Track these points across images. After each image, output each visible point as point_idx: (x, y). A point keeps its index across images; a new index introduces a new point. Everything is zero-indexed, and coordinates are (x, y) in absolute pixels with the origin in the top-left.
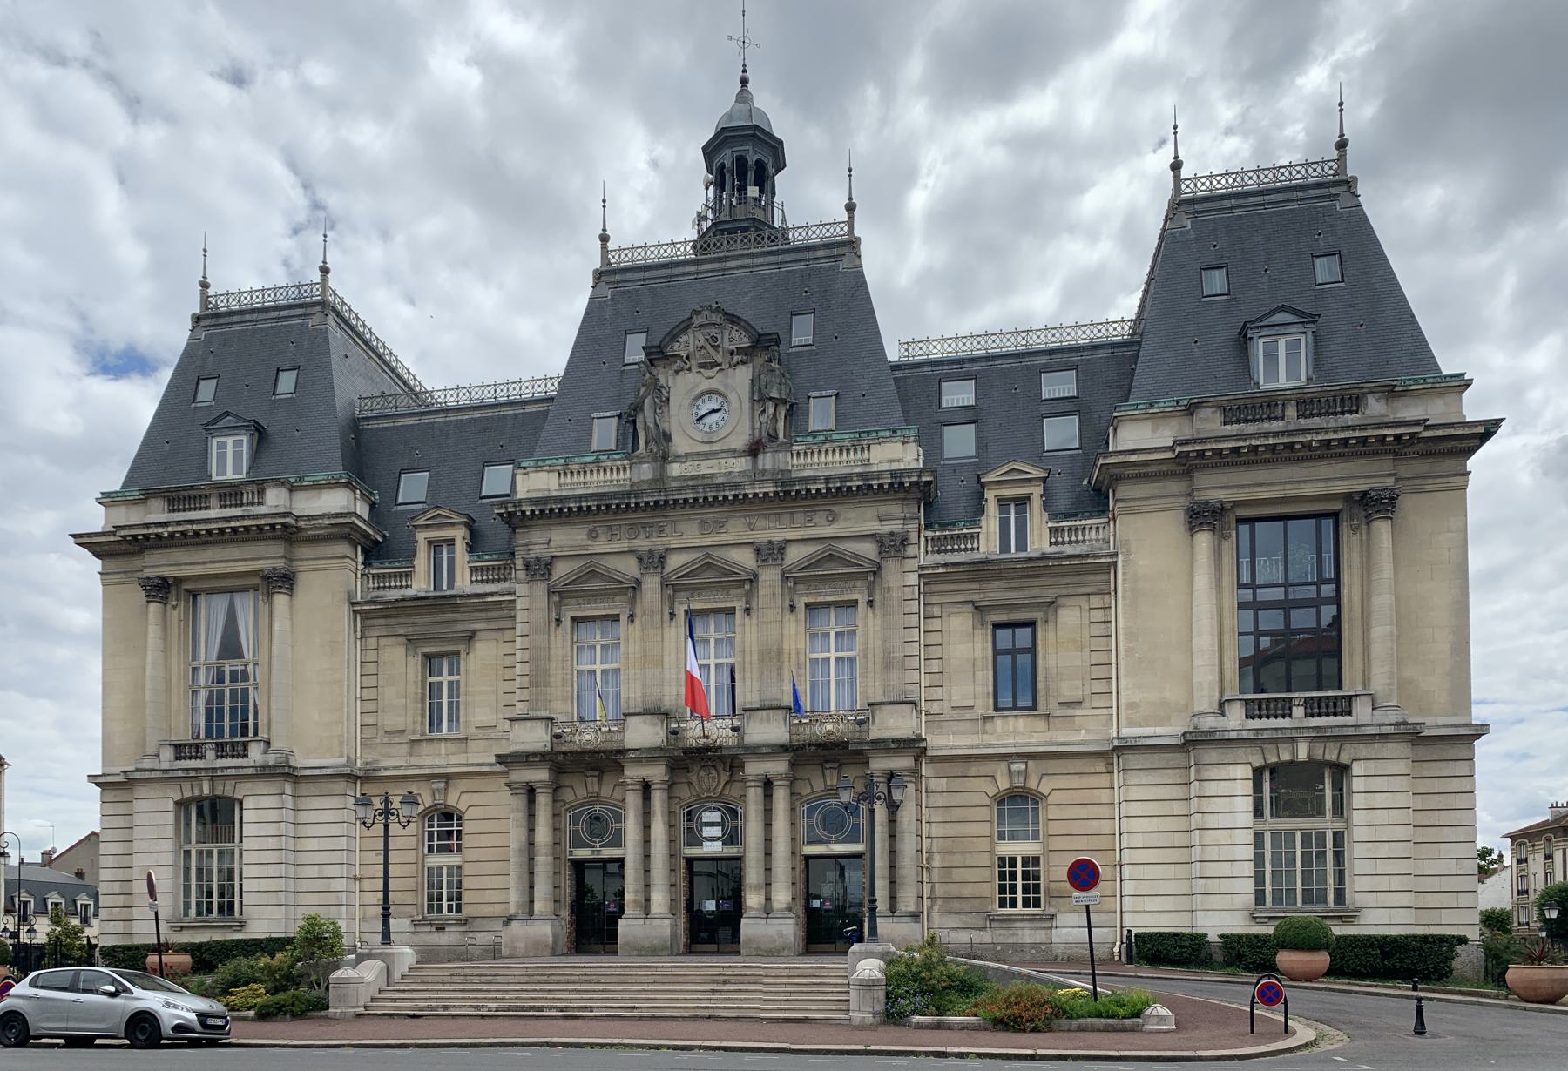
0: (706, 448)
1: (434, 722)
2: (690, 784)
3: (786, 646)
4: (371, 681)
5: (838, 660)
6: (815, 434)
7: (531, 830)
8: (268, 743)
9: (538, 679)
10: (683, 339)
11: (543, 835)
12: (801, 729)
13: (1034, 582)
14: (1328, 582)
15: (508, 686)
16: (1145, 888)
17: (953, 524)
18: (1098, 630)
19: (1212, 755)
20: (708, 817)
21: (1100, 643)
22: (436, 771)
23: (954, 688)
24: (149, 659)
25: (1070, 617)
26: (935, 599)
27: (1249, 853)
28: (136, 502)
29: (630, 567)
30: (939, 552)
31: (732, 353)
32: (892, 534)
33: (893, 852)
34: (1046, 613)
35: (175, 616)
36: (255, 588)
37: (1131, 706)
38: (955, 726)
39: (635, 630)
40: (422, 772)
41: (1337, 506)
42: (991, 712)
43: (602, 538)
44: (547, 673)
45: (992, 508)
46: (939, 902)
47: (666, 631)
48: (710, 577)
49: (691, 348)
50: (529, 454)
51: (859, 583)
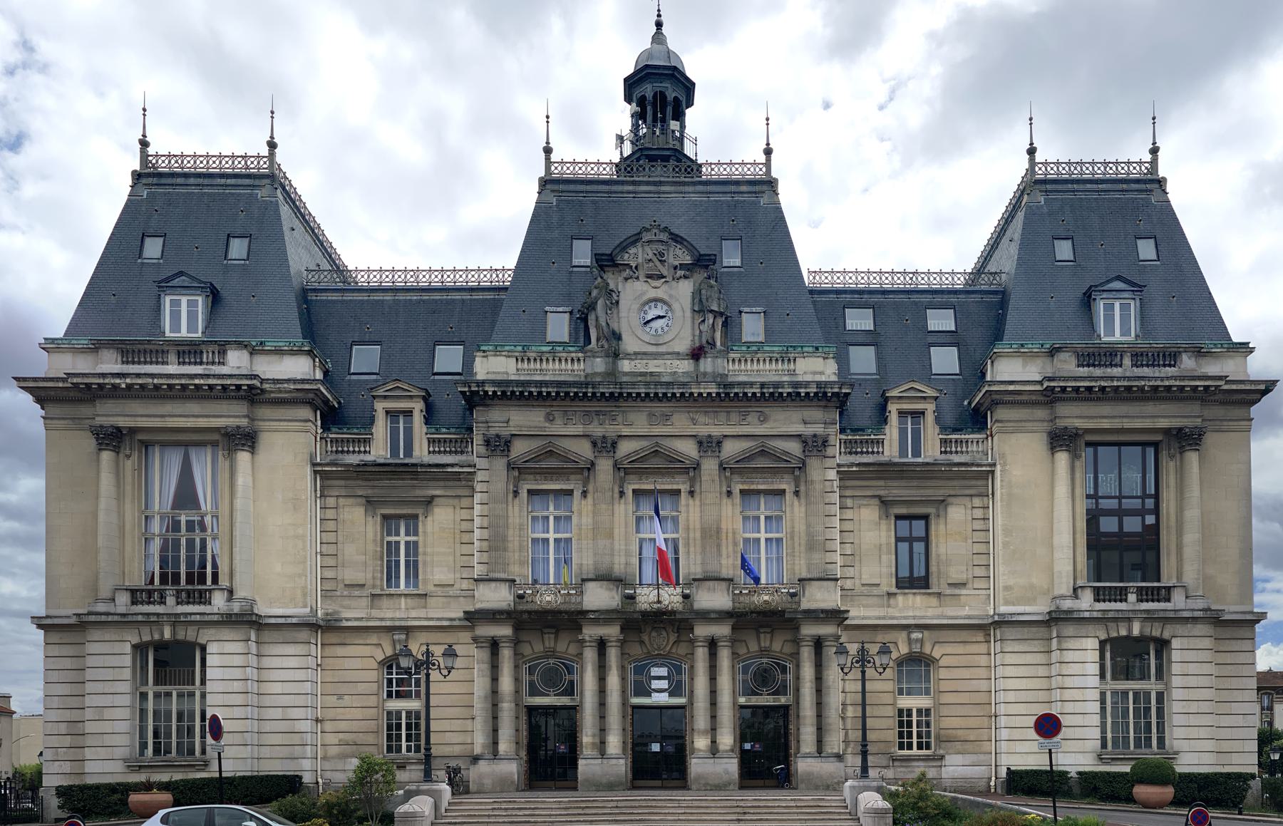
1: (392, 577)
2: (642, 642)
3: (724, 526)
4: (331, 537)
5: (767, 540)
7: (495, 679)
8: (231, 592)
10: (632, 251)
12: (742, 599)
13: (929, 483)
14: (1150, 496)
17: (863, 430)
18: (978, 525)
19: (1069, 630)
20: (655, 671)
21: (979, 536)
22: (397, 623)
23: (864, 569)
24: (103, 504)
25: (958, 514)
26: (848, 493)
27: (1096, 707)
28: (83, 351)
29: (584, 450)
30: (850, 453)
31: (675, 268)
32: (815, 436)
33: (819, 705)
34: (938, 509)
35: (129, 463)
36: (214, 444)
37: (1007, 588)
38: (865, 601)
40: (383, 624)
41: (1158, 437)
42: (894, 590)
43: (559, 421)
44: (504, 539)
45: (894, 418)
46: (852, 745)
47: (616, 506)
48: (656, 463)
49: (640, 260)
50: (487, 340)
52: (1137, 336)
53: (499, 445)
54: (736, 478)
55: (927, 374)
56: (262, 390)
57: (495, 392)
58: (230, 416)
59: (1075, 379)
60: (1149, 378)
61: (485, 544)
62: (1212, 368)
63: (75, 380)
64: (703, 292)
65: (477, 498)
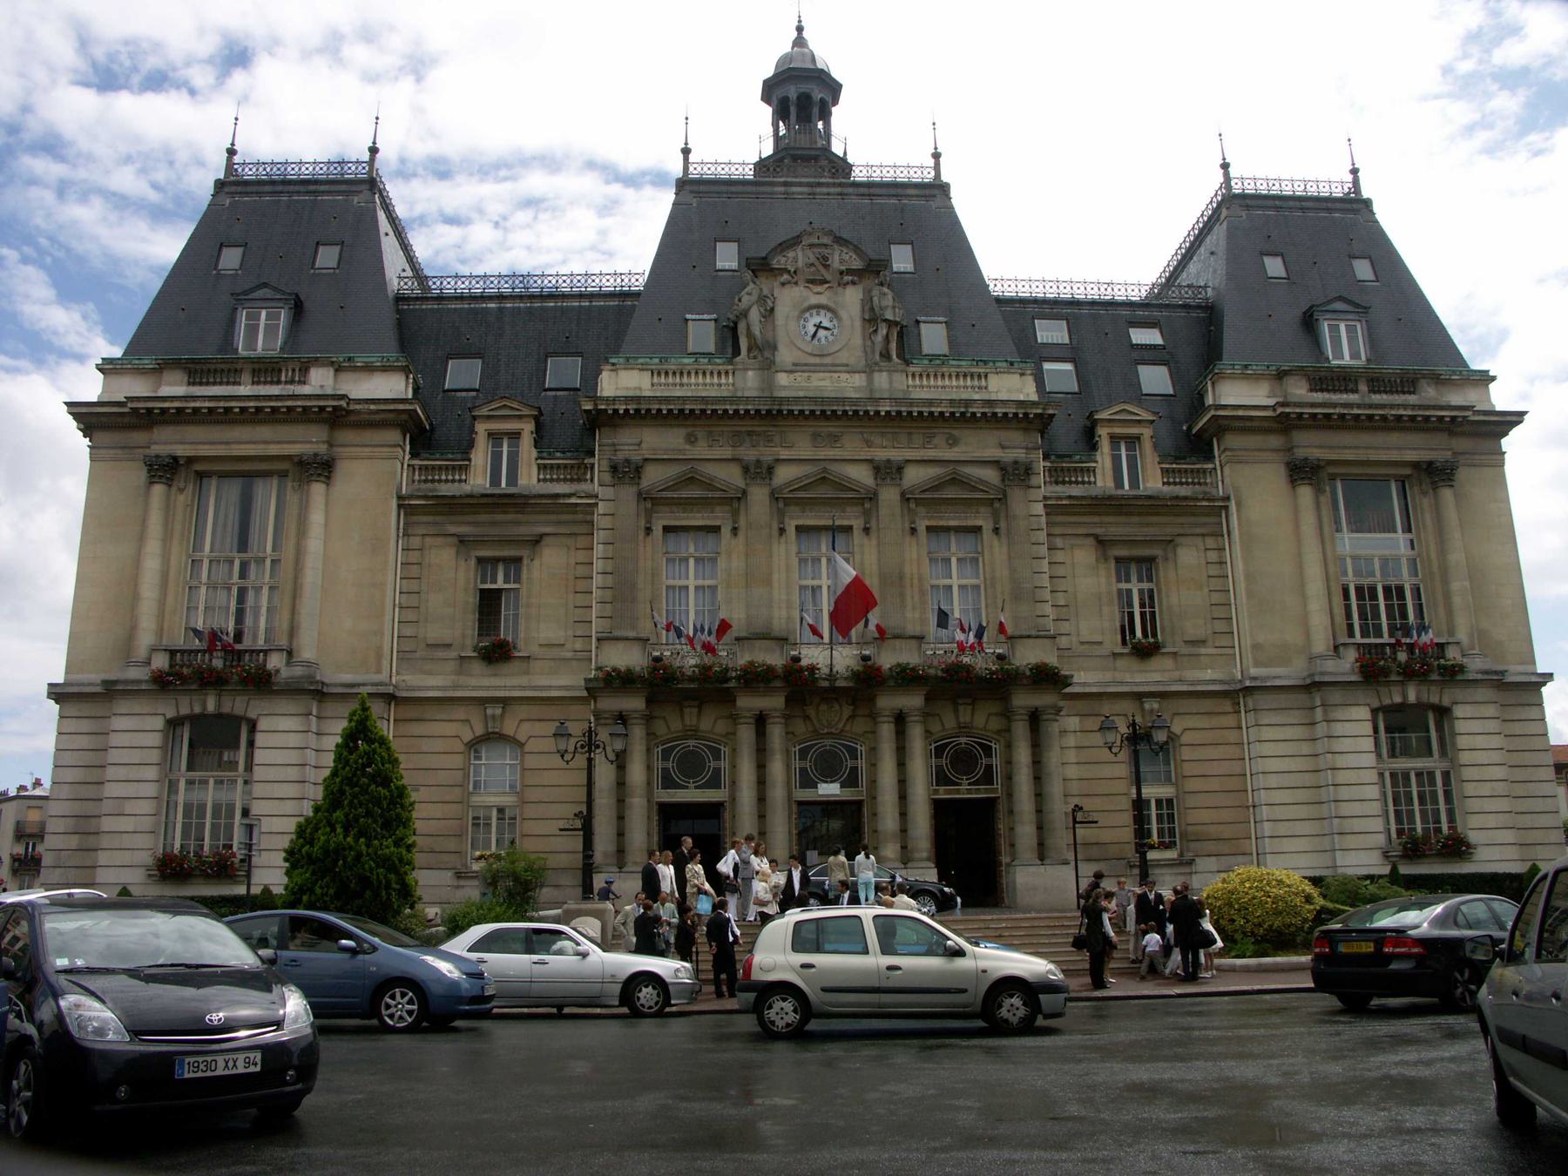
0: (817, 360)
3: (907, 570)
4: (414, 585)
6: (932, 358)
8: (290, 653)
9: (622, 592)
10: (791, 254)
11: (636, 772)
15: (581, 599)
16: (1282, 829)
18: (1214, 570)
25: (1189, 556)
26: (1057, 530)
29: (731, 476)
30: (1057, 483)
31: (841, 273)
32: (1016, 462)
35: (181, 498)
36: (283, 475)
39: (739, 543)
43: (702, 443)
45: (1105, 446)
47: (775, 546)
49: (800, 264)
50: (616, 351)
51: (982, 509)
52: (1368, 360)
53: (627, 472)
54: (922, 511)
55: (1140, 398)
56: (349, 412)
57: (626, 411)
58: (307, 441)
59: (1313, 405)
60: (1392, 407)
61: (609, 593)
62: (1456, 398)
63: (135, 405)
64: (876, 299)
65: (600, 535)
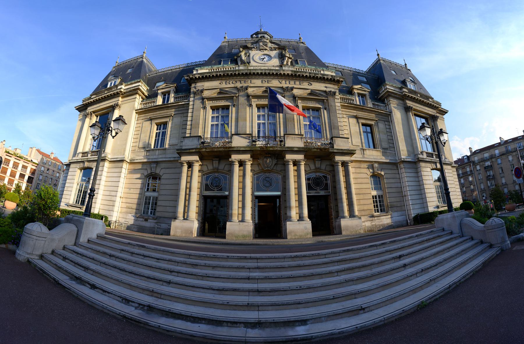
22: (154, 160)
